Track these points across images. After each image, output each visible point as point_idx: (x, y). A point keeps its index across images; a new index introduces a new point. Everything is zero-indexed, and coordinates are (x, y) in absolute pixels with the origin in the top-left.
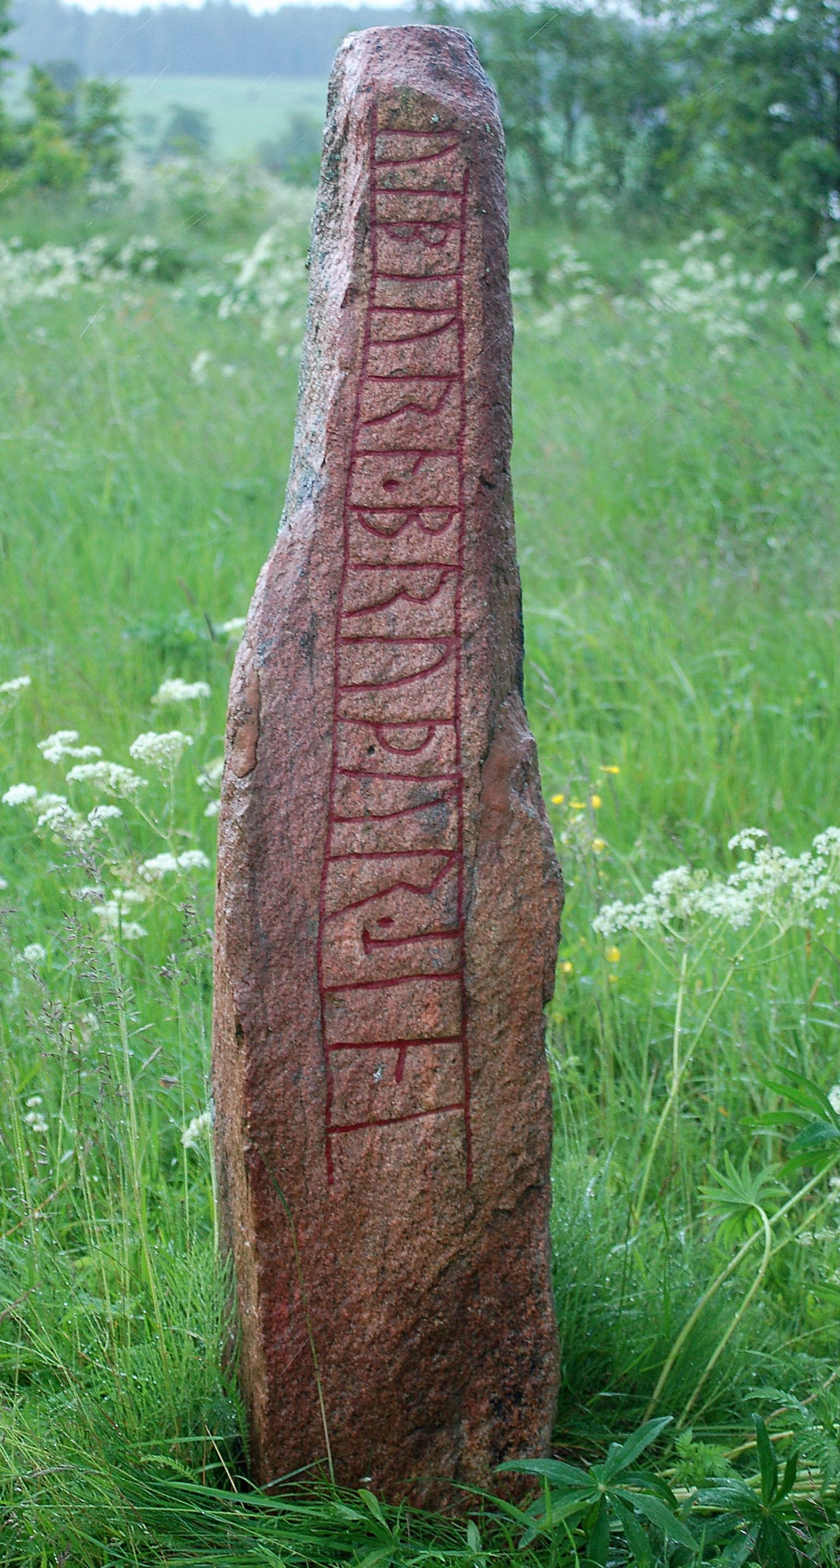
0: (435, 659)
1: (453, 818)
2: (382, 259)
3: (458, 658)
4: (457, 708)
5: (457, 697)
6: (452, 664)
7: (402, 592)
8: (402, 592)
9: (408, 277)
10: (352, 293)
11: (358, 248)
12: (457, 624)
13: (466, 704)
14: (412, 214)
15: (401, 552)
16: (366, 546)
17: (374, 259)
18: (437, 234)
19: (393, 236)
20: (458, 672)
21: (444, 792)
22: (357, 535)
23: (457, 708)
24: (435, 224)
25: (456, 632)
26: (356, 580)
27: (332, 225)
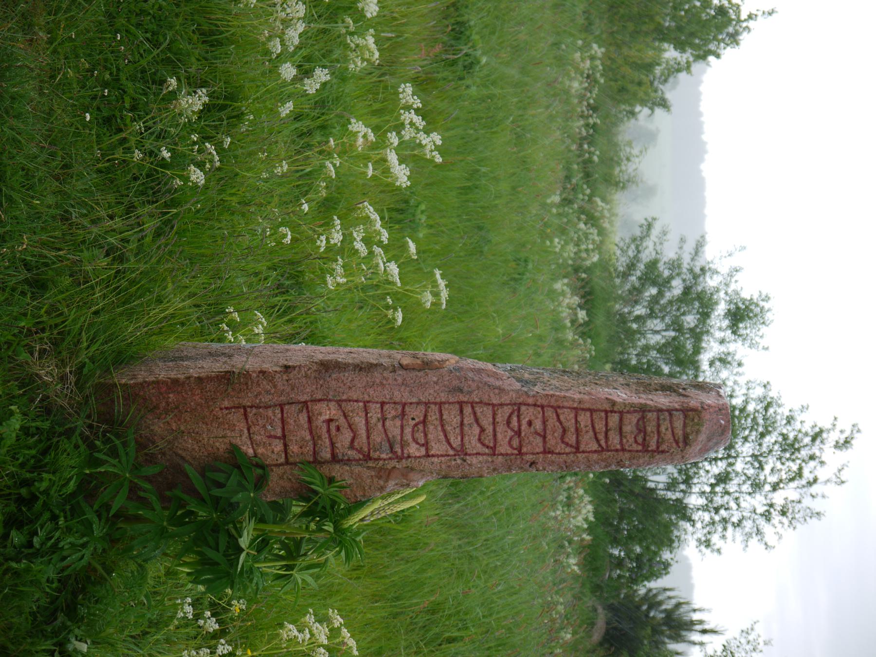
0: (454, 446)
1: (384, 456)
2: (629, 416)
3: (455, 455)
4: (433, 456)
5: (438, 456)
6: (451, 452)
7: (483, 430)
8: (483, 430)
9: (621, 429)
10: (613, 403)
11: (632, 405)
12: (470, 455)
13: (435, 460)
14: (649, 429)
15: (500, 428)
16: (502, 414)
17: (628, 412)
18: (640, 439)
19: (638, 421)
20: (448, 456)
21: (396, 452)
22: (507, 410)
23: (433, 456)
24: (644, 439)
25: (466, 454)
26: (488, 411)
27: (642, 389)
